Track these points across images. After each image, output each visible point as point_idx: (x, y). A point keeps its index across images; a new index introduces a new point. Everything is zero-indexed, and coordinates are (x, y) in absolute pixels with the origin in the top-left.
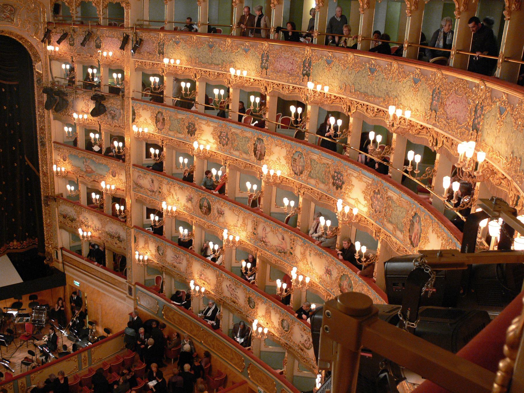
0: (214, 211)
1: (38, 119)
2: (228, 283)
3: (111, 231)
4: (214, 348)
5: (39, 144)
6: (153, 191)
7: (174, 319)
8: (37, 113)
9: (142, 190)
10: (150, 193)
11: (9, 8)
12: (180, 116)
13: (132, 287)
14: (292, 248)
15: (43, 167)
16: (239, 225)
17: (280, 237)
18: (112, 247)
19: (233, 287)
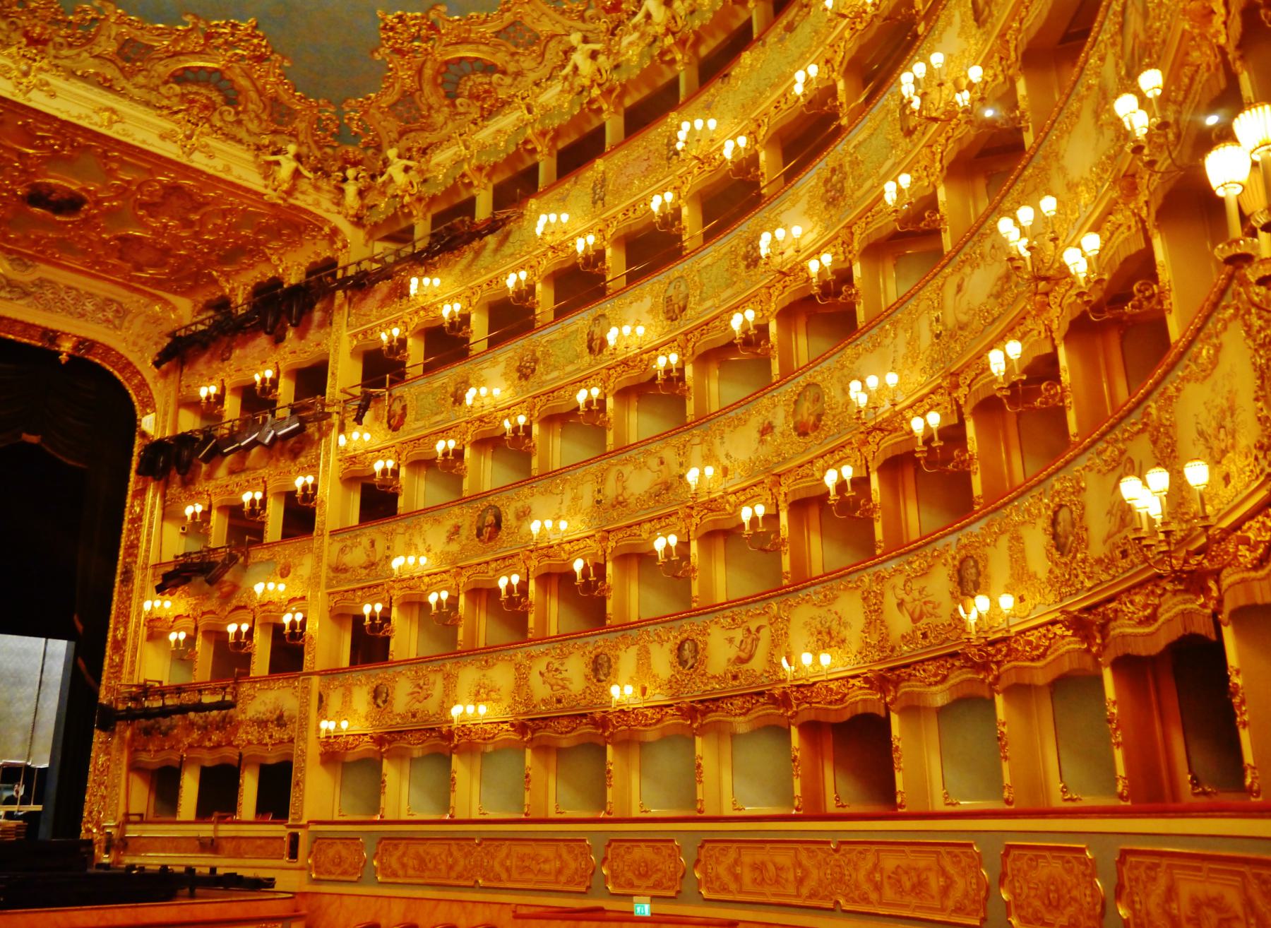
0: (509, 517)
1: (126, 526)
2: (541, 665)
3: (262, 709)
4: (510, 879)
5: (118, 579)
6: (373, 564)
7: (404, 866)
8: (127, 517)
9: (348, 575)
10: (364, 572)
11: (115, 307)
12: (435, 385)
13: (301, 832)
14: (681, 464)
15: (116, 629)
16: (564, 512)
17: (653, 462)
18: (259, 751)
19: (556, 665)
